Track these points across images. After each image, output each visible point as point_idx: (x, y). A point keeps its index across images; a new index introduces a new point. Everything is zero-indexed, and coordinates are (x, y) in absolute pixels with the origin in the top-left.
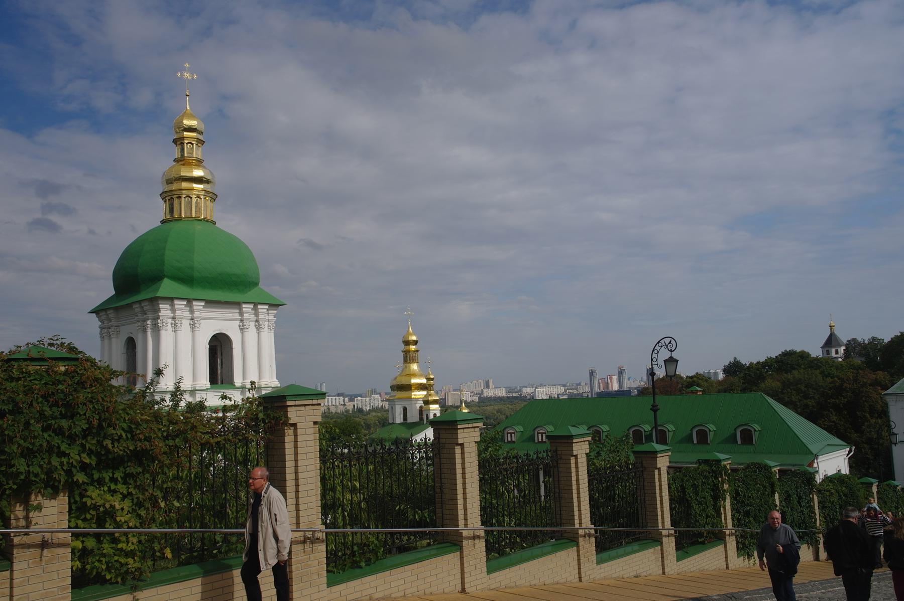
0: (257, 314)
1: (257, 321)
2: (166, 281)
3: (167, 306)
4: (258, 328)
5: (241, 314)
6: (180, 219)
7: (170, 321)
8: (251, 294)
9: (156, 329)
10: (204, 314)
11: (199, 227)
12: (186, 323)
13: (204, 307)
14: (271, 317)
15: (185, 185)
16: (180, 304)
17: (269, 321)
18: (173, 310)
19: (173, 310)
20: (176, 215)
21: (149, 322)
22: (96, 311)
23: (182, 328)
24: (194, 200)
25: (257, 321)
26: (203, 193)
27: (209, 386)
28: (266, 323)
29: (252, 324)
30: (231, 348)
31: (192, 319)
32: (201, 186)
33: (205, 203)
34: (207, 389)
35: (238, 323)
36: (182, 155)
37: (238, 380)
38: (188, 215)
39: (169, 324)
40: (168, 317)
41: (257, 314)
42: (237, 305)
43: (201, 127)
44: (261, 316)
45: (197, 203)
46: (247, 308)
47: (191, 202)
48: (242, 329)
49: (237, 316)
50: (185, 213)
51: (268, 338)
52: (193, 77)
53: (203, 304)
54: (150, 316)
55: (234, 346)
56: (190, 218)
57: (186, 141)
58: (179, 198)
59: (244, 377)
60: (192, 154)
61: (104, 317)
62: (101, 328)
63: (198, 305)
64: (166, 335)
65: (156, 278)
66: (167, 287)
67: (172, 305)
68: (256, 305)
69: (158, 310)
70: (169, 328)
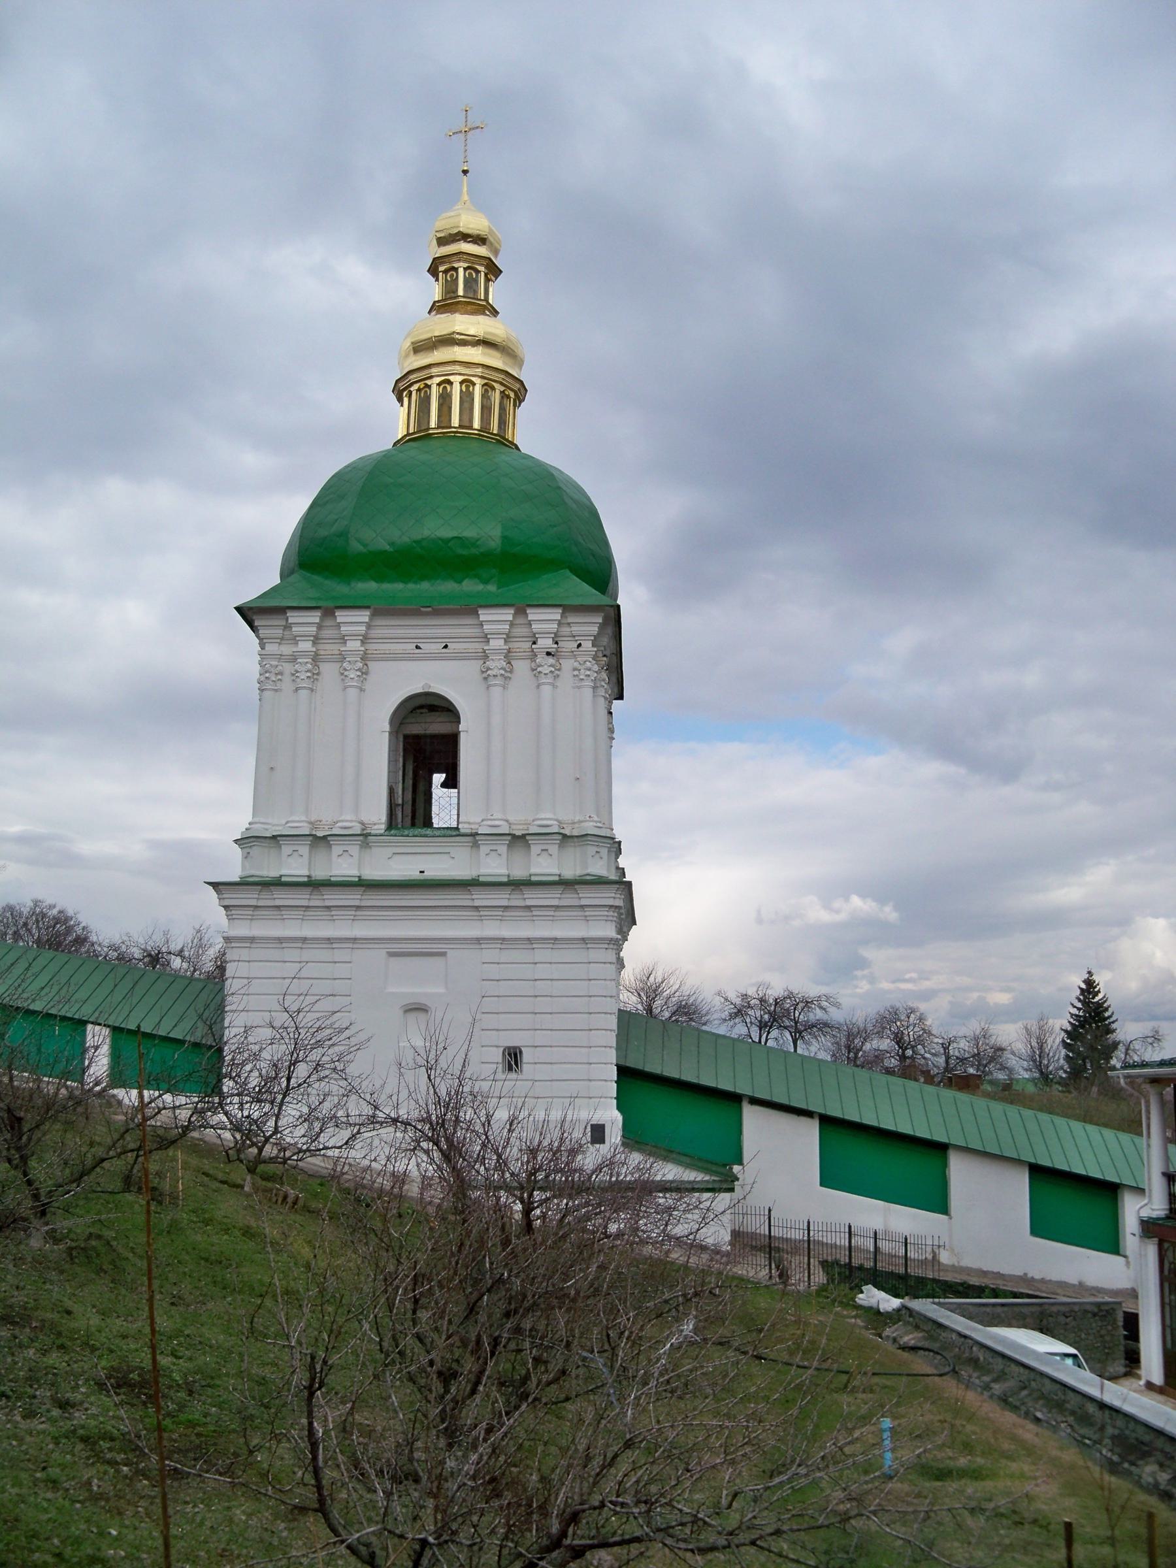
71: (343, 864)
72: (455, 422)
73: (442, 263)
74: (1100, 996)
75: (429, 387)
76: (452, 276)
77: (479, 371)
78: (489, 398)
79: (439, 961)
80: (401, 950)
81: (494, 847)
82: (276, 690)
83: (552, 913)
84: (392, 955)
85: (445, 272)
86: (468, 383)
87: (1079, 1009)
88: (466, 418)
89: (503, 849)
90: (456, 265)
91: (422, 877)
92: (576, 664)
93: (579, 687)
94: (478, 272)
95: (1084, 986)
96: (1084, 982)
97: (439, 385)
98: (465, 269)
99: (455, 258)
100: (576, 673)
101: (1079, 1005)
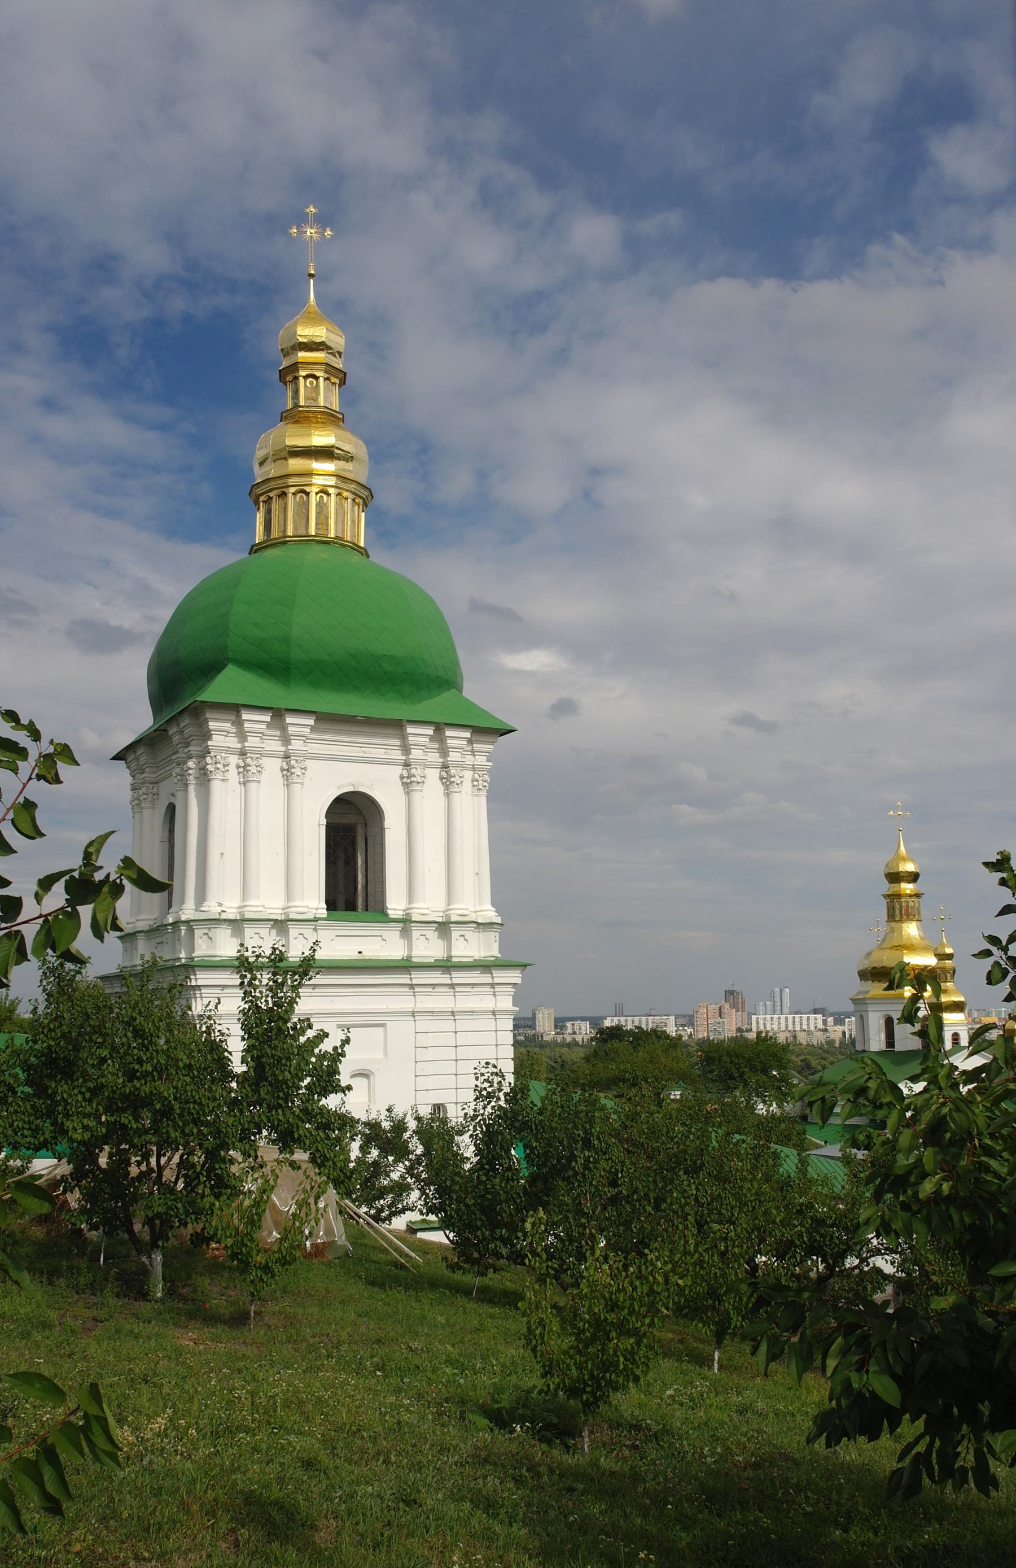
0: (444, 752)
1: (445, 767)
2: (231, 671)
3: (227, 726)
4: (447, 782)
5: (406, 749)
6: (283, 542)
7: (234, 760)
8: (436, 705)
9: (204, 777)
10: (314, 748)
11: (320, 553)
12: (273, 766)
13: (313, 729)
14: (481, 760)
15: (295, 464)
16: (255, 721)
17: (473, 768)
18: (242, 736)
19: (242, 736)
20: (275, 534)
21: (191, 764)
23: (263, 778)
24: (314, 499)
25: (445, 767)
26: (332, 481)
27: (323, 912)
28: (468, 775)
29: (433, 775)
30: (382, 829)
31: (287, 757)
32: (329, 466)
33: (339, 508)
34: (316, 920)
35: (399, 770)
37: (395, 904)
38: (302, 532)
39: (233, 771)
40: (229, 750)
41: (444, 752)
42: (396, 726)
43: (338, 341)
44: (454, 756)
45: (321, 507)
46: (419, 735)
47: (306, 505)
48: (408, 784)
49: (397, 755)
50: (295, 528)
51: (472, 809)
54: (194, 749)
56: (305, 540)
57: (303, 373)
58: (283, 495)
60: (316, 400)
61: (133, 765)
62: (134, 788)
63: (299, 725)
64: (225, 792)
65: (211, 669)
66: (229, 683)
67: (239, 723)
68: (439, 728)
69: (207, 735)
70: (233, 775)
73: (306, 368)
75: (308, 494)
76: (311, 383)
77: (353, 487)
78: (343, 507)
81: (423, 933)
82: (223, 780)
83: (470, 989)
85: (306, 377)
88: (340, 529)
90: (318, 374)
91: (357, 956)
92: (477, 776)
93: (477, 796)
97: (317, 494)
98: (326, 379)
100: (476, 783)
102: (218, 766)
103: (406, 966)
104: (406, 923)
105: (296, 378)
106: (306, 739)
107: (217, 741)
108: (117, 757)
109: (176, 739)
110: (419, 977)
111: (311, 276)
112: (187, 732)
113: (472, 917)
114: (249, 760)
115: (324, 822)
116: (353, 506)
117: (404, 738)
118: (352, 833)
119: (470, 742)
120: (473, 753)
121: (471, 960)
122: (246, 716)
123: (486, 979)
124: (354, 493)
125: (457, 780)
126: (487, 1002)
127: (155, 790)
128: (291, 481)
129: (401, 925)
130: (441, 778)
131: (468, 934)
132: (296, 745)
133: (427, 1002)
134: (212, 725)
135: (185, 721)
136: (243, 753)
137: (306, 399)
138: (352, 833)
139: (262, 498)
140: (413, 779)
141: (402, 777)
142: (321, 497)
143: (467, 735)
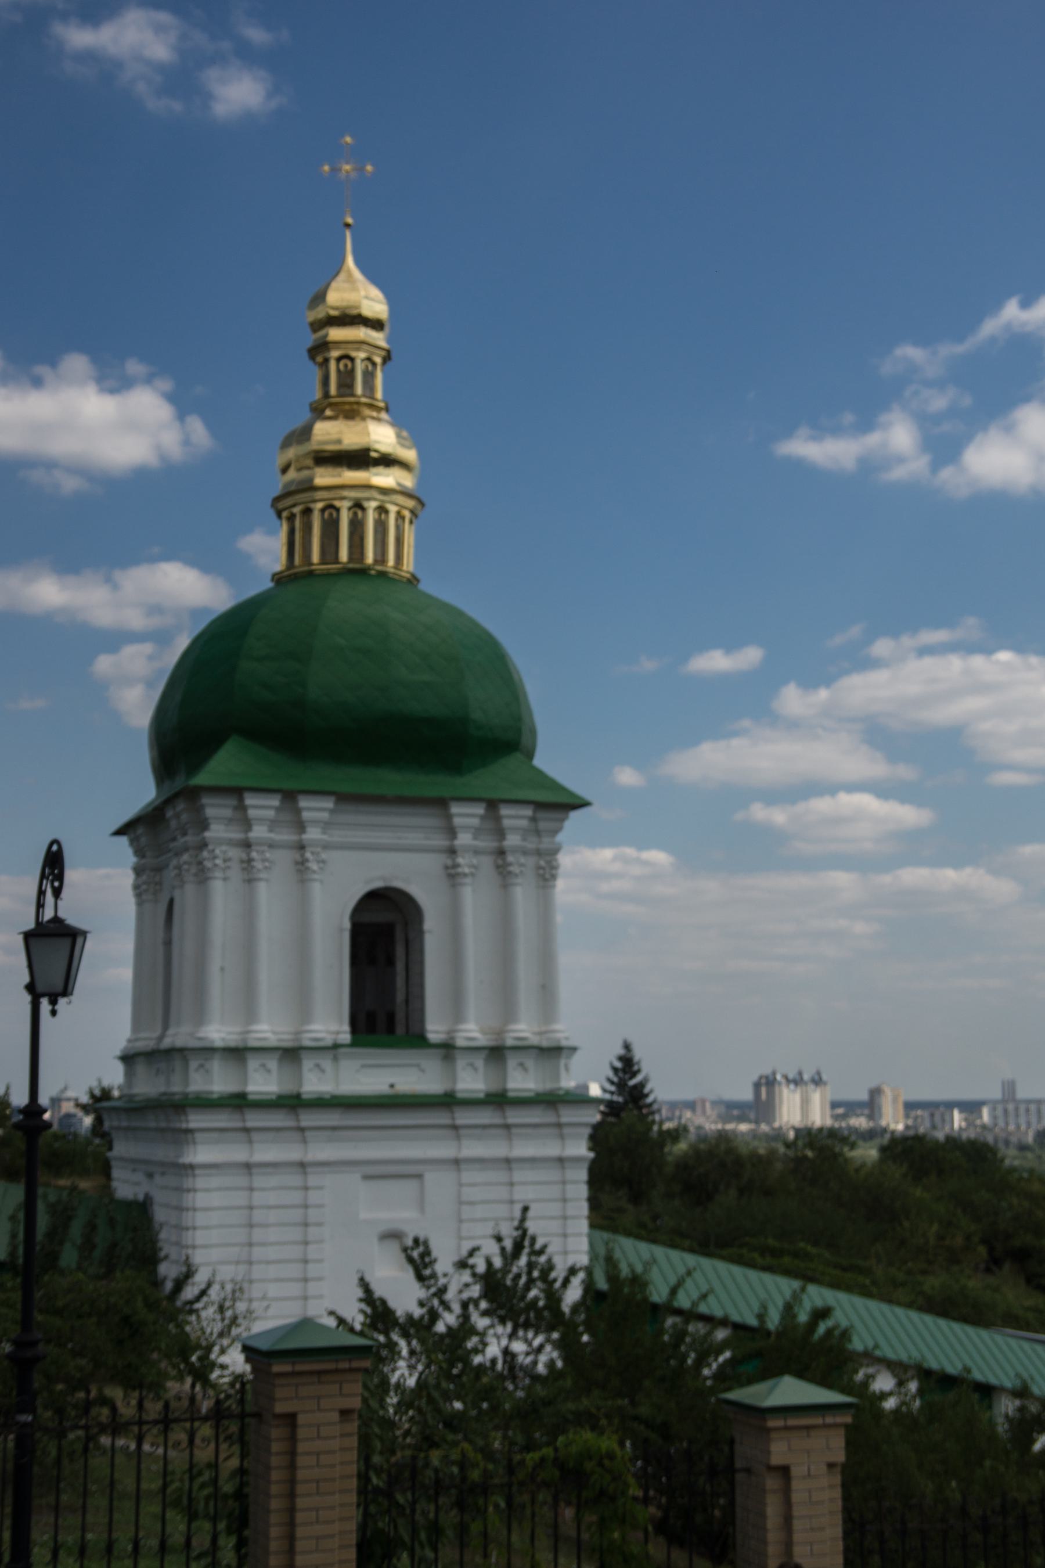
0: (500, 833)
1: (501, 852)
4: (504, 872)
7: (236, 853)
10: (337, 836)
16: (262, 807)
22: (119, 832)
27: (346, 1037)
30: (421, 933)
34: (336, 1046)
35: (443, 859)
36: (326, 395)
40: (231, 843)
42: (441, 803)
44: (512, 840)
46: (467, 816)
48: (452, 876)
52: (361, 170)
53: (329, 803)
55: (428, 924)
57: (335, 354)
58: (308, 512)
59: (458, 1014)
63: (315, 809)
64: (223, 895)
68: (492, 805)
71: (316, 1082)
72: (370, 558)
73: (338, 348)
74: (639, 1078)
75: (338, 510)
79: (411, 1185)
80: (378, 1173)
84: (367, 1177)
85: (339, 359)
86: (382, 510)
87: (612, 1093)
89: (480, 1063)
94: (374, 364)
95: (619, 1065)
96: (621, 1058)
99: (350, 346)
100: (541, 872)
101: (613, 1088)
102: (218, 861)
103: (448, 1101)
104: (448, 1049)
105: (326, 361)
106: (326, 826)
107: (216, 831)
108: (119, 832)
109: (173, 824)
110: (464, 1117)
111: (348, 225)
112: (184, 817)
113: (535, 1040)
114: (254, 855)
115: (347, 925)
116: (396, 520)
117: (449, 817)
118: (383, 938)
119: (533, 819)
120: (538, 833)
121: (531, 1094)
122: (250, 800)
123: (549, 1117)
124: (397, 504)
125: (515, 869)
126: (552, 1149)
127: (157, 879)
128: (319, 495)
129: (442, 1051)
130: (498, 867)
131: (530, 1063)
132: (313, 834)
133: (472, 1148)
134: (210, 812)
135: (181, 805)
136: (247, 845)
137: (340, 385)
138: (383, 938)
139: (285, 514)
140: (460, 870)
141: (447, 867)
142: (355, 514)
143: (528, 812)
